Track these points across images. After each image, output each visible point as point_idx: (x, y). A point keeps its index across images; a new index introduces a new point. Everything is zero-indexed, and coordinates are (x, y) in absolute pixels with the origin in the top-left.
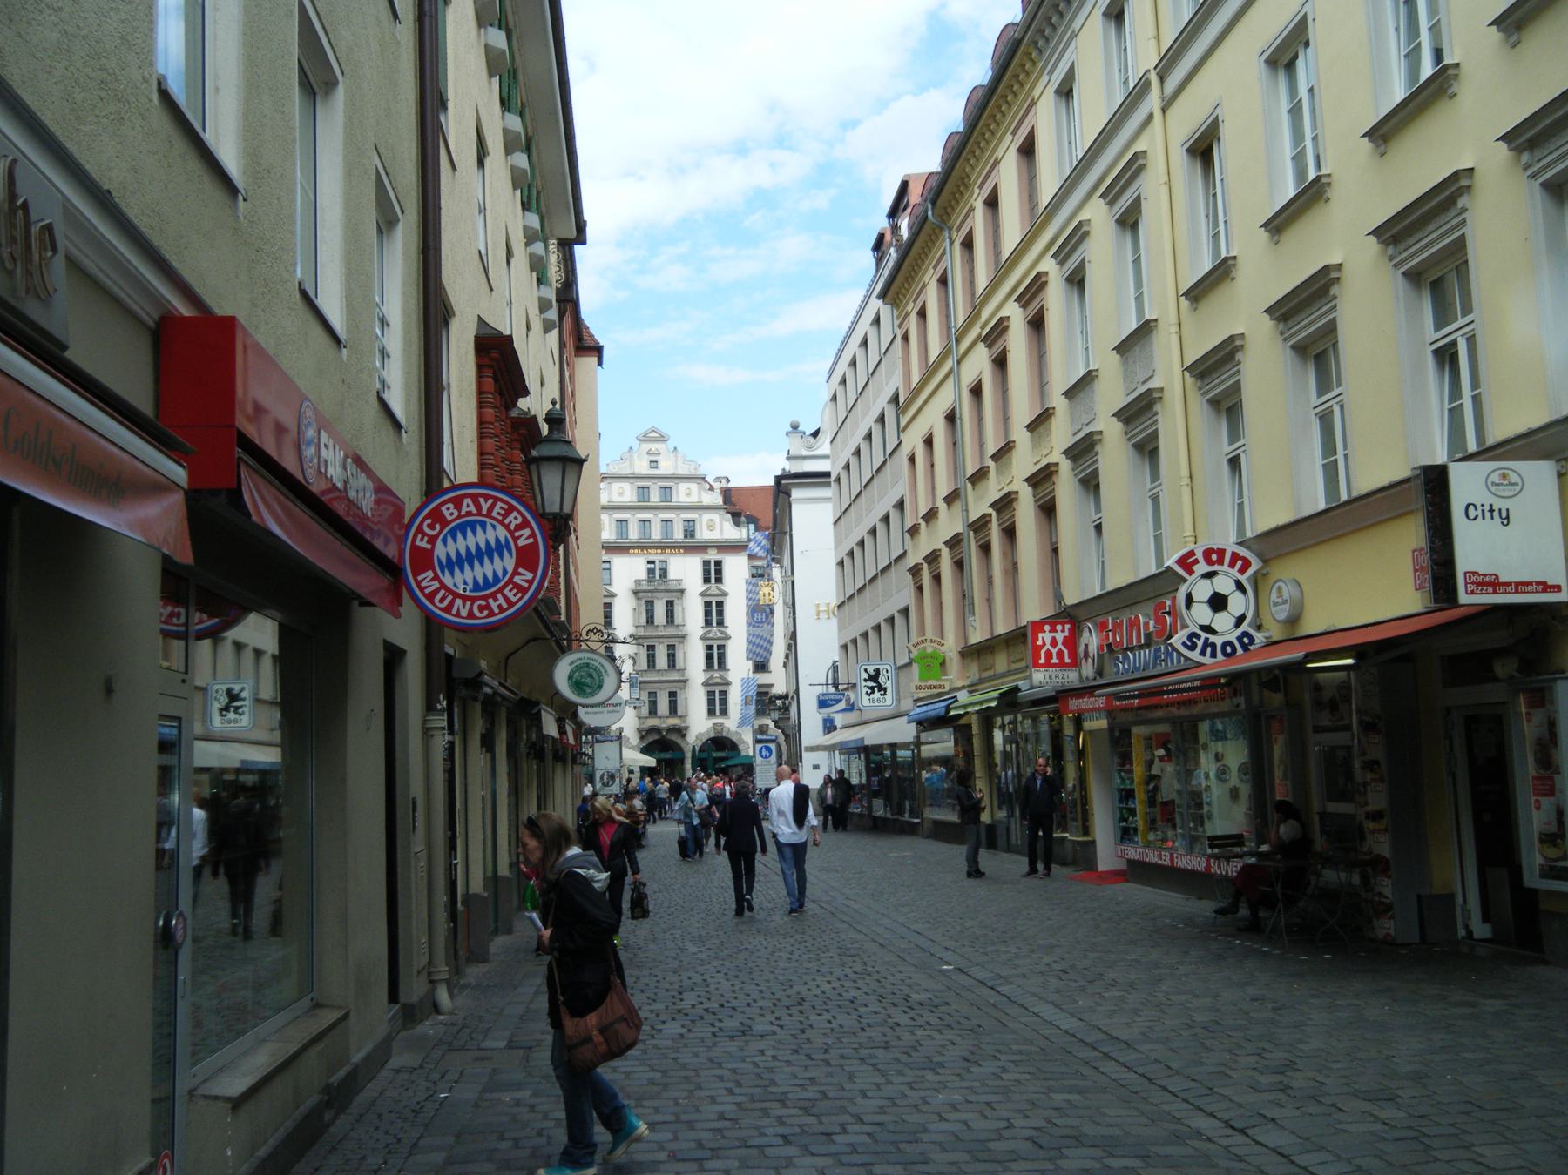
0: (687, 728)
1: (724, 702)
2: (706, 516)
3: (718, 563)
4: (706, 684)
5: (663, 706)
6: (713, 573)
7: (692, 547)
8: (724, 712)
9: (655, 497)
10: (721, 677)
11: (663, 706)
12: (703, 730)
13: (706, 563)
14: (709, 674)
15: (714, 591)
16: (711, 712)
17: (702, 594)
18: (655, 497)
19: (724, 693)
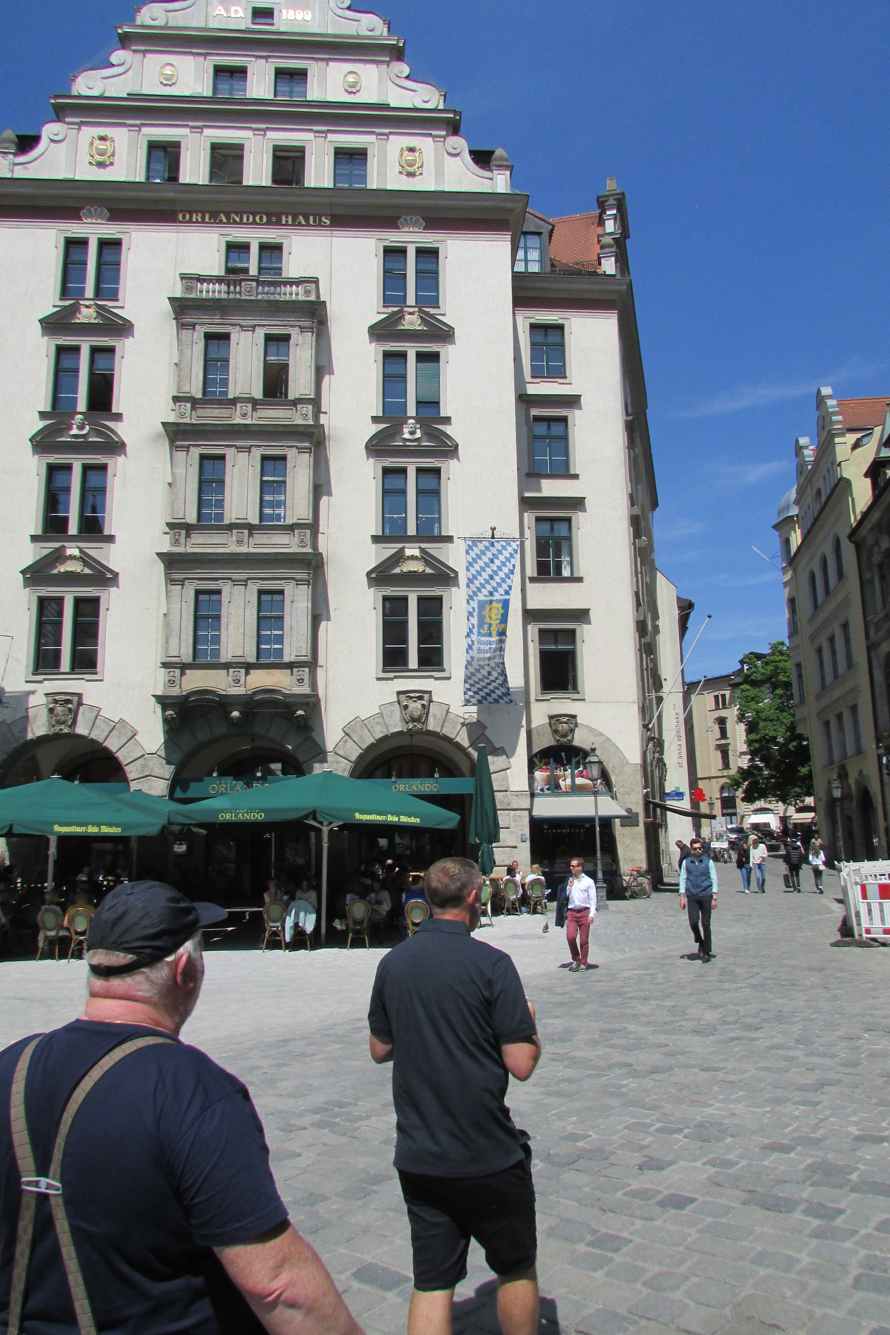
0: (312, 704)
1: (432, 632)
2: (398, 142)
3: (428, 254)
4: (380, 576)
5: (237, 634)
6: (410, 280)
7: (356, 209)
8: (432, 659)
9: (260, 83)
10: (426, 558)
11: (237, 634)
12: (368, 710)
13: (393, 253)
14: (389, 550)
15: (412, 322)
16: (394, 659)
17: (378, 332)
18: (260, 83)
19: (432, 610)
